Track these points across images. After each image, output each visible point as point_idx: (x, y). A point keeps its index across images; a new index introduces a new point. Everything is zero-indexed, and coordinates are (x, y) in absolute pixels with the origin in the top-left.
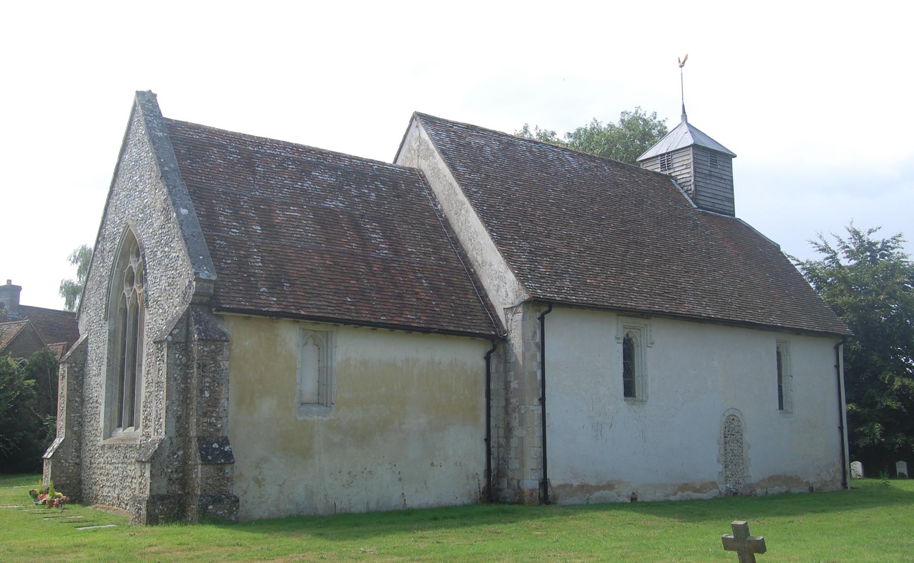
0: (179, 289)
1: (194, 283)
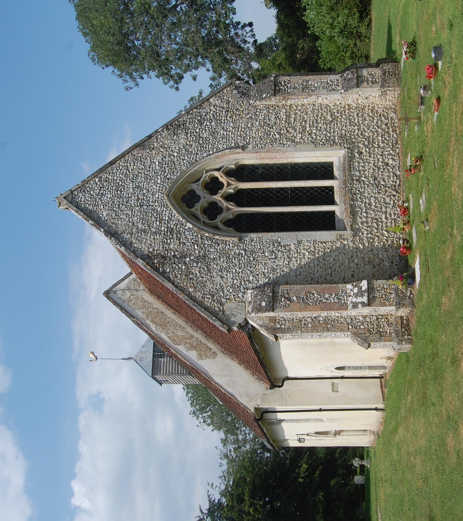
0: (238, 102)
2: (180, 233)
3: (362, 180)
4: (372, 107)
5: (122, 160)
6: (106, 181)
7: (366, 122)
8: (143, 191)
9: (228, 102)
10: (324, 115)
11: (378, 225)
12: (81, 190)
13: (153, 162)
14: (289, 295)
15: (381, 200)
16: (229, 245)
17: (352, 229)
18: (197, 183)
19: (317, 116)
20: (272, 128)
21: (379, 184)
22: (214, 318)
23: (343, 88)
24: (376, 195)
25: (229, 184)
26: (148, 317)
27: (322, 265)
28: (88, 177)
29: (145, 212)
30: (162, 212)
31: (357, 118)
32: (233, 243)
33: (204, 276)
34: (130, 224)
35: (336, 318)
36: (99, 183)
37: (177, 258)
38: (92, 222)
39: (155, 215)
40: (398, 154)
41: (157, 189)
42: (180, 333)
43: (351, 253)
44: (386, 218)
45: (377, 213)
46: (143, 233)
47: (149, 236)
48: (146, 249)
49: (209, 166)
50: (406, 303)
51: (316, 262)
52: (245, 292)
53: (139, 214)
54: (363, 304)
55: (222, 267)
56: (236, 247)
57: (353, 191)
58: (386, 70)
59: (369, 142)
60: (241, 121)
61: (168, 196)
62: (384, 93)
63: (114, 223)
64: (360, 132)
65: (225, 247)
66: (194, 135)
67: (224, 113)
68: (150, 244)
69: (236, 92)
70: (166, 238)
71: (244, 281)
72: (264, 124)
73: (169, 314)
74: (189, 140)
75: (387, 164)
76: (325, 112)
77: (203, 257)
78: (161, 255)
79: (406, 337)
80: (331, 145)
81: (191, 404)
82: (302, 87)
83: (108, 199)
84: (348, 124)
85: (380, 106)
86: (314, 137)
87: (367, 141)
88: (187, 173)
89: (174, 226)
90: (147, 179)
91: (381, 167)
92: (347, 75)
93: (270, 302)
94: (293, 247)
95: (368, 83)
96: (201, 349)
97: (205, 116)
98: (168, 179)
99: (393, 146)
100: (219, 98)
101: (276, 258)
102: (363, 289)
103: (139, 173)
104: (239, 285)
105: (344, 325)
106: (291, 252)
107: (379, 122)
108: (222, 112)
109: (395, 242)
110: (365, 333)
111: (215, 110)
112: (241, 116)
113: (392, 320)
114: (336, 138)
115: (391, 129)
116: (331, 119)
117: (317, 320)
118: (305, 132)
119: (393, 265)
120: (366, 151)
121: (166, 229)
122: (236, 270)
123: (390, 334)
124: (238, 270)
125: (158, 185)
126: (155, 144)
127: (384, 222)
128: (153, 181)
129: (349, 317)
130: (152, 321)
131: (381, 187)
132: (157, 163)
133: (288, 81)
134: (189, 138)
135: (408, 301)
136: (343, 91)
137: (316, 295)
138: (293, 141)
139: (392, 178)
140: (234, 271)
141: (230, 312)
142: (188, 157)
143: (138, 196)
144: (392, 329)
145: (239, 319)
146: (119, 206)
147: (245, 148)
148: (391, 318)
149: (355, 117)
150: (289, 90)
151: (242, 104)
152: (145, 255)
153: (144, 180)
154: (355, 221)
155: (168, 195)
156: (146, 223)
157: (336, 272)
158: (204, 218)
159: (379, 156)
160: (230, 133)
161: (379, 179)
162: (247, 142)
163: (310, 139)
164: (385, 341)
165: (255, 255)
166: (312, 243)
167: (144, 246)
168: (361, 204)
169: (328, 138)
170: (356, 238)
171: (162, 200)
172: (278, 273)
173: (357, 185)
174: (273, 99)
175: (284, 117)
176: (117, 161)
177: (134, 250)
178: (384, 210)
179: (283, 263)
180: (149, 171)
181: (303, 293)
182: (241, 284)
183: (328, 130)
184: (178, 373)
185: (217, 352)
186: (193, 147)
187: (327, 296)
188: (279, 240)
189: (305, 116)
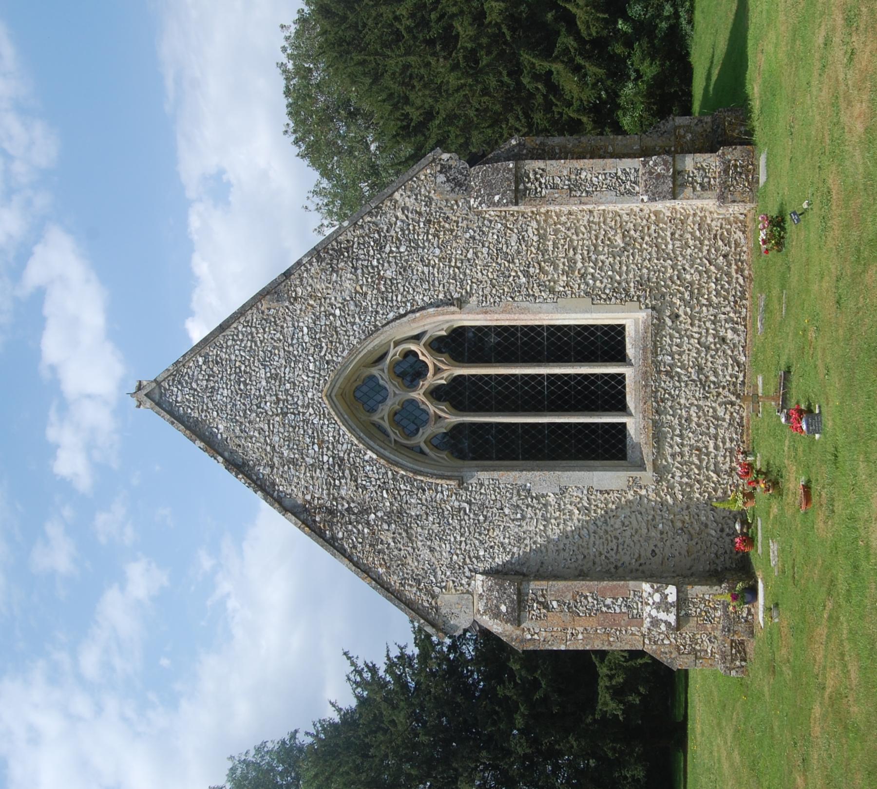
0: (447, 201)
1: (445, 156)
2: (356, 468)
4: (701, 218)
5: (242, 320)
6: (217, 363)
7: (689, 251)
8: (285, 385)
9: (429, 202)
10: (610, 236)
11: (701, 461)
12: (173, 380)
13: (298, 326)
14: (545, 598)
15: (708, 411)
16: (442, 492)
17: (656, 468)
18: (380, 367)
19: (597, 238)
20: (513, 262)
21: (706, 382)
23: (647, 191)
24: (701, 403)
25: (437, 370)
27: (601, 533)
28: (184, 356)
29: (292, 426)
30: (322, 428)
31: (671, 242)
32: (448, 489)
34: (268, 448)
37: (354, 514)
38: (202, 445)
39: (310, 432)
40: (745, 319)
41: (309, 382)
43: (652, 512)
44: (716, 448)
45: (700, 437)
47: (303, 472)
48: (300, 495)
50: (740, 629)
51: (592, 528)
53: (282, 430)
55: (431, 531)
56: (454, 497)
57: (659, 394)
58: (730, 161)
60: (454, 245)
61: (329, 397)
63: (239, 446)
65: (436, 496)
67: (422, 225)
68: (306, 487)
70: (332, 477)
71: (469, 557)
72: (497, 254)
74: (361, 282)
75: (723, 340)
76: (611, 228)
77: (399, 513)
79: (738, 663)
80: (621, 300)
82: (569, 185)
83: (225, 399)
84: (654, 255)
86: (591, 282)
87: (688, 293)
88: (360, 352)
91: (712, 346)
92: (656, 164)
93: (513, 610)
94: (552, 499)
95: (694, 189)
97: (388, 231)
99: (735, 302)
100: (411, 191)
101: (523, 518)
103: (274, 348)
104: (461, 564)
105: (637, 637)
106: (549, 508)
107: (713, 250)
108: (418, 222)
110: (671, 653)
111: (405, 218)
112: (454, 234)
114: (632, 285)
115: (734, 267)
118: (573, 272)
119: (724, 535)
120: (686, 313)
121: (331, 459)
122: (455, 538)
123: (711, 655)
124: (458, 537)
125: (310, 374)
126: (299, 290)
131: (709, 387)
132: (305, 330)
133: (541, 172)
134: (360, 278)
137: (590, 599)
138: (552, 291)
139: (730, 368)
140: (452, 539)
141: (448, 610)
142: (360, 318)
143: (276, 395)
144: (715, 646)
146: (245, 413)
149: (669, 239)
151: (455, 207)
152: (299, 506)
153: (284, 363)
154: (661, 451)
156: (295, 447)
157: (625, 546)
159: (708, 324)
162: (467, 292)
163: (582, 286)
165: (488, 512)
166: (585, 492)
167: (295, 490)
168: (673, 419)
169: (616, 285)
170: (662, 485)
171: (320, 403)
172: (526, 545)
173: (667, 383)
175: (535, 238)
177: (279, 496)
178: (712, 431)
179: (536, 528)
180: (292, 345)
181: (570, 596)
182: (464, 563)
183: (617, 267)
186: (369, 298)
187: (609, 601)
188: (528, 485)
189: (575, 237)
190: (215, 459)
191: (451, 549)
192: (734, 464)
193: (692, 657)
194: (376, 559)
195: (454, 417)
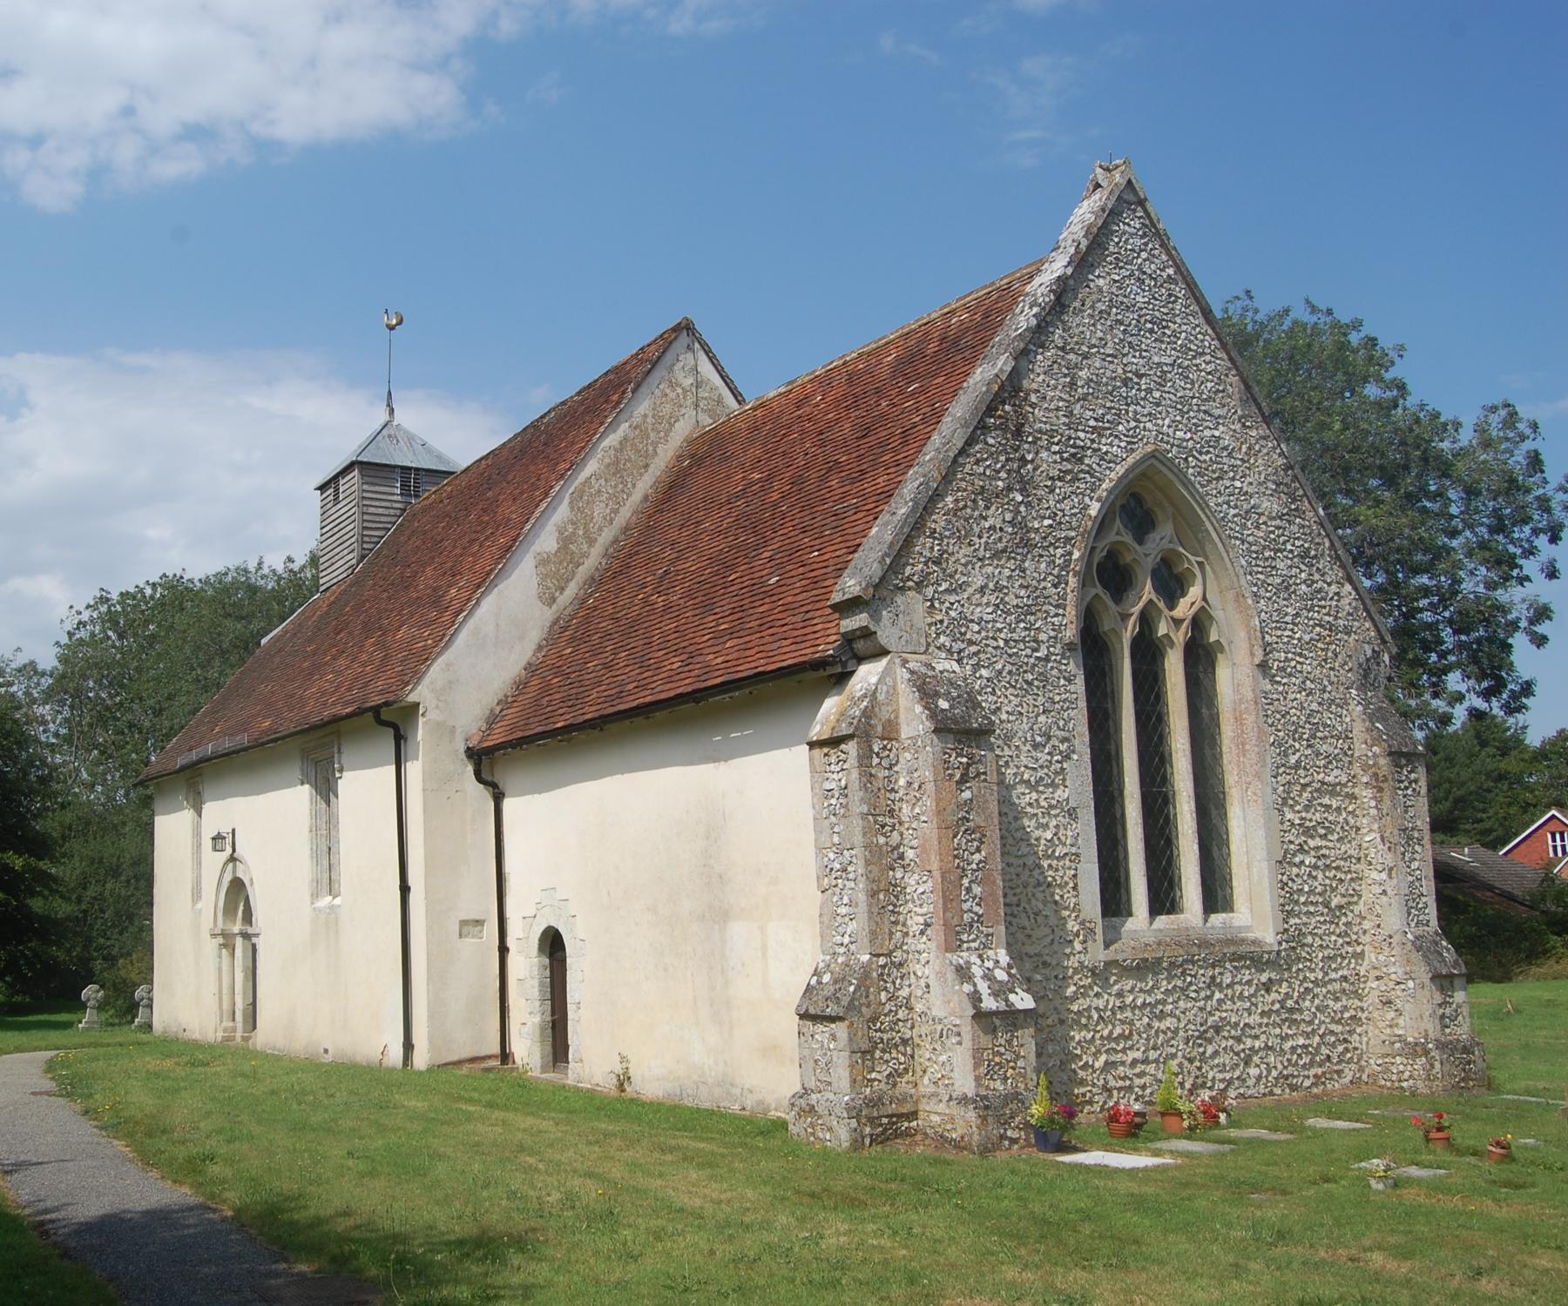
2: (1073, 481)
3: (1213, 993)
4: (1360, 1018)
5: (1215, 342)
6: (1170, 296)
8: (1158, 390)
11: (1116, 1040)
12: (1146, 226)
13: (1218, 423)
14: (974, 778)
15: (1172, 1046)
16: (1057, 615)
17: (1108, 964)
19: (1337, 868)
20: (1309, 746)
21: (1206, 1039)
22: (888, 561)
24: (1181, 1033)
25: (1177, 622)
26: (635, 428)
28: (1175, 248)
29: (1113, 391)
30: (1116, 436)
31: (1338, 976)
32: (1061, 625)
33: (983, 541)
34: (1085, 349)
35: (901, 918)
36: (1165, 275)
37: (1020, 468)
41: (1163, 426)
42: (599, 510)
43: (1054, 963)
44: (1134, 1062)
45: (1144, 1036)
46: (1068, 380)
47: (1063, 395)
48: (1034, 386)
49: (1214, 572)
51: (1030, 861)
52: (952, 654)
53: (1108, 374)
54: (975, 998)
55: (1006, 591)
56: (1052, 634)
57: (1191, 967)
59: (1291, 1010)
61: (1152, 455)
62: (1415, 1050)
63: (1083, 305)
64: (1311, 985)
65: (1051, 604)
66: (1279, 536)
68: (1045, 398)
69: (1369, 653)
70: (1060, 441)
71: (979, 651)
72: (1314, 724)
73: (644, 485)
74: (1269, 523)
75: (1247, 1063)
76: (1347, 890)
77: (1028, 541)
78: (1023, 425)
79: (868, 1130)
80: (1283, 905)
81: (128, 593)
83: (1133, 296)
85: (1365, 1039)
88: (1203, 509)
89: (1088, 465)
90: (1181, 403)
91: (1242, 1046)
94: (1061, 794)
96: (560, 563)
98: (1186, 459)
99: (1287, 1078)
101: (1036, 746)
102: (1012, 997)
103: (1193, 383)
104: (968, 636)
105: (887, 943)
106: (1051, 790)
107: (1333, 1039)
108: (1328, 614)
109: (1082, 1090)
110: (868, 1006)
113: (903, 1086)
114: (1297, 921)
115: (1320, 1071)
116: (1333, 905)
117: (895, 860)
118: (1304, 833)
120: (1273, 1003)
121: (1082, 444)
122: (1000, 630)
123: (868, 1080)
124: (1002, 635)
125: (1171, 430)
127: (1125, 1058)
128: (1178, 418)
129: (905, 956)
130: (625, 438)
131: (1200, 1045)
135: (995, 1132)
136: (1410, 936)
137: (977, 857)
139: (1220, 1076)
140: (999, 625)
141: (902, 608)
142: (1235, 516)
144: (882, 1086)
145: (886, 634)
146: (1122, 323)
147: (1264, 671)
148: (907, 1083)
149: (1340, 973)
150: (1400, 792)
152: (1020, 381)
153: (1179, 395)
154: (1126, 974)
155: (1154, 456)
156: (1091, 391)
158: (1102, 551)
160: (1290, 633)
161: (1217, 1039)
163: (1292, 846)
164: (852, 1066)
165: (1038, 688)
166: (1074, 850)
167: (1040, 379)
168: (1162, 990)
170: (1087, 977)
171: (1141, 439)
173: (1203, 979)
174: (1374, 749)
176: (1213, 329)
177: (1031, 350)
178: (1153, 1055)
179: (1026, 767)
181: (980, 821)
182: (971, 643)
183: (1312, 898)
184: (364, 528)
185: (554, 607)
187: (977, 890)
188: (1075, 757)
189: (1336, 836)
190: (1069, 263)
191: (986, 622)
192: (1115, 1092)
193: (864, 1047)
194: (965, 494)
195: (1129, 643)
